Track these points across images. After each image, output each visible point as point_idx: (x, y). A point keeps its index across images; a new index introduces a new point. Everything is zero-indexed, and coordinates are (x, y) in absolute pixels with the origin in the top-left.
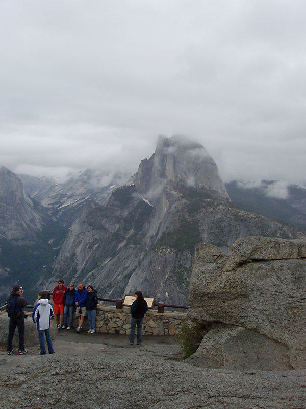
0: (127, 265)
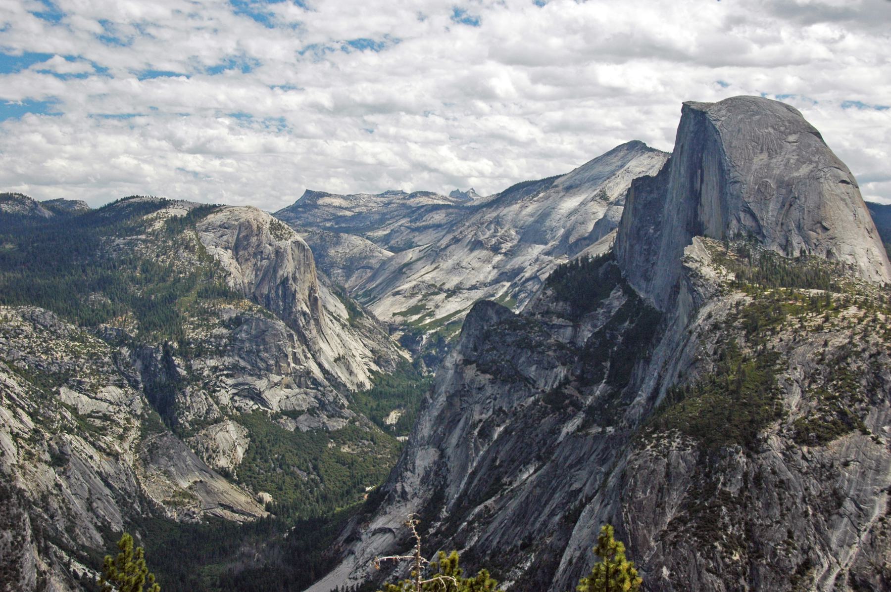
0: (576, 486)
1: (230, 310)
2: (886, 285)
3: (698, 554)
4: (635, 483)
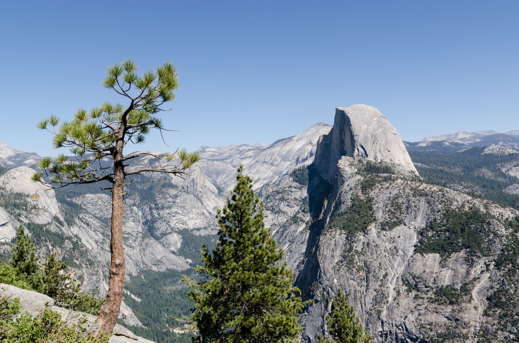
1: (173, 192)
2: (411, 171)
3: (347, 273)
4: (323, 248)
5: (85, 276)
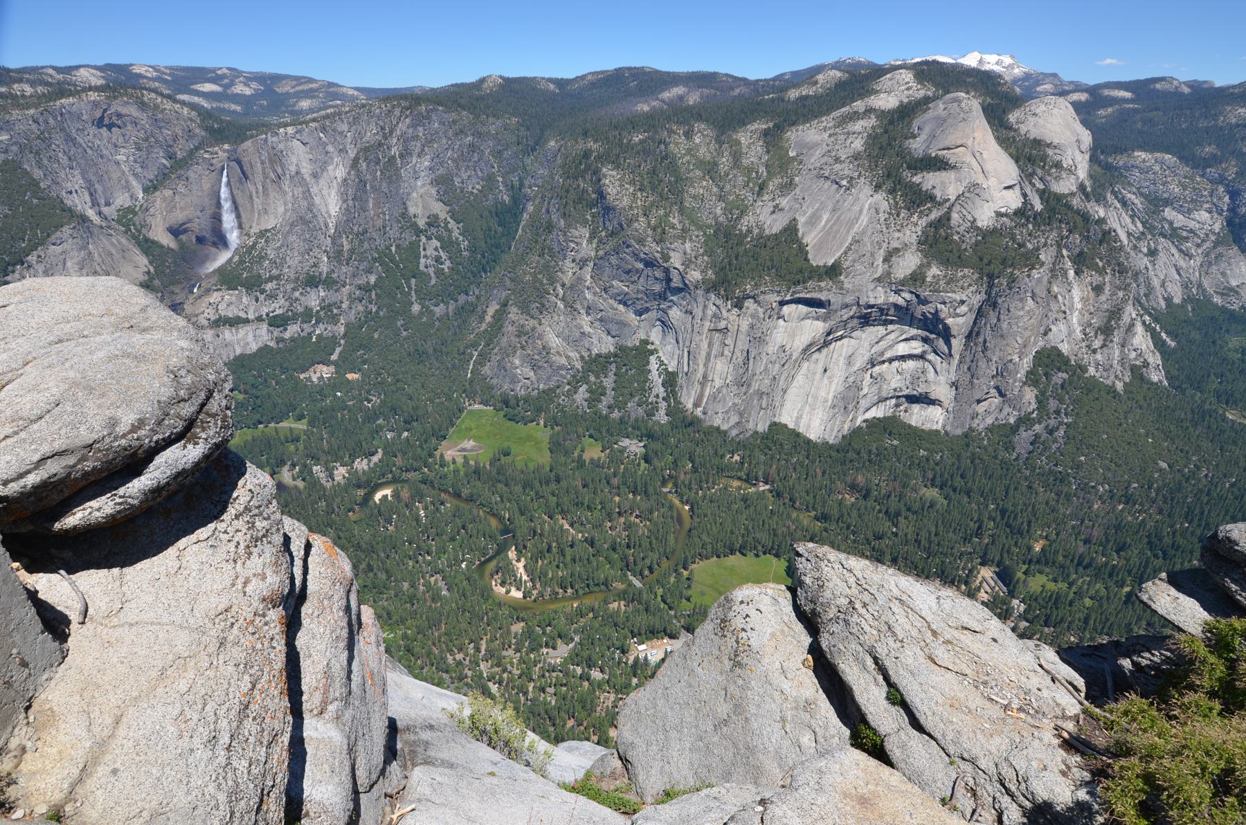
5: (1107, 288)
